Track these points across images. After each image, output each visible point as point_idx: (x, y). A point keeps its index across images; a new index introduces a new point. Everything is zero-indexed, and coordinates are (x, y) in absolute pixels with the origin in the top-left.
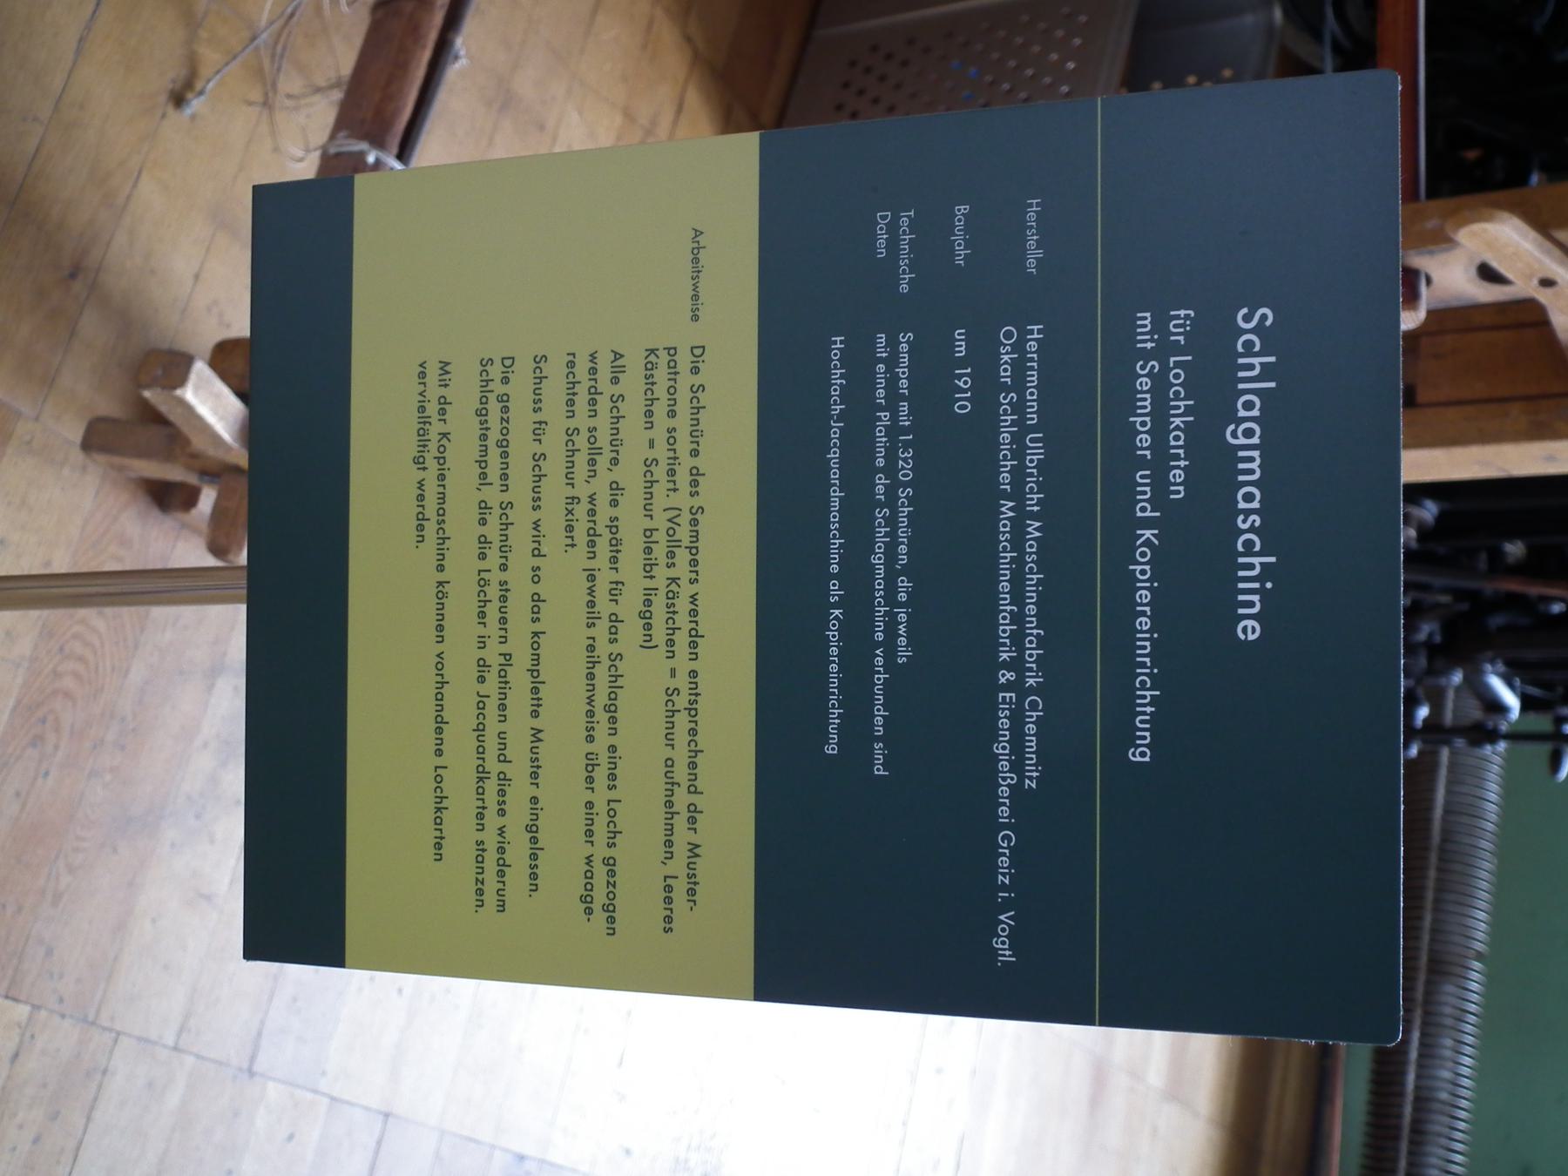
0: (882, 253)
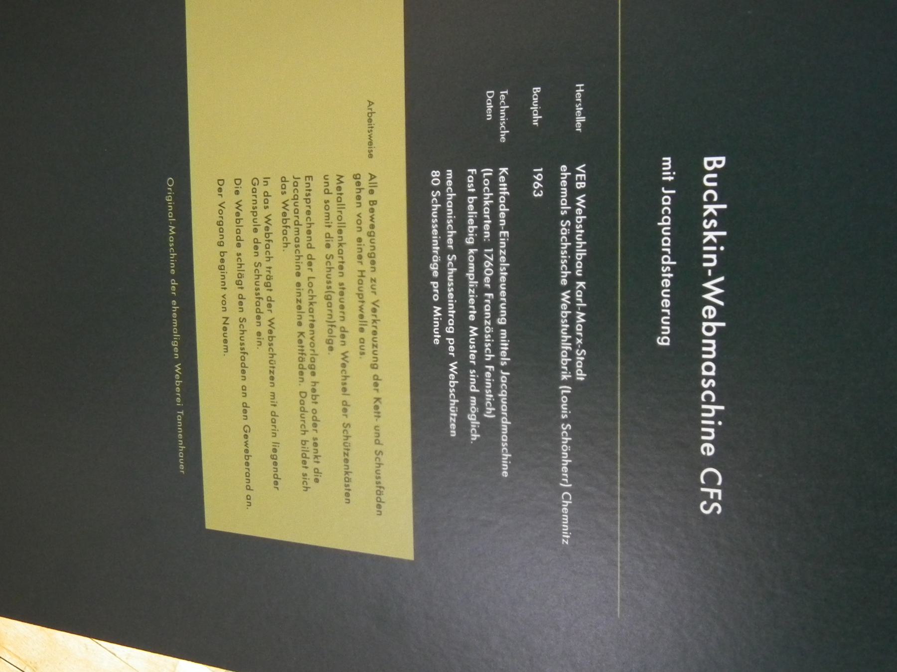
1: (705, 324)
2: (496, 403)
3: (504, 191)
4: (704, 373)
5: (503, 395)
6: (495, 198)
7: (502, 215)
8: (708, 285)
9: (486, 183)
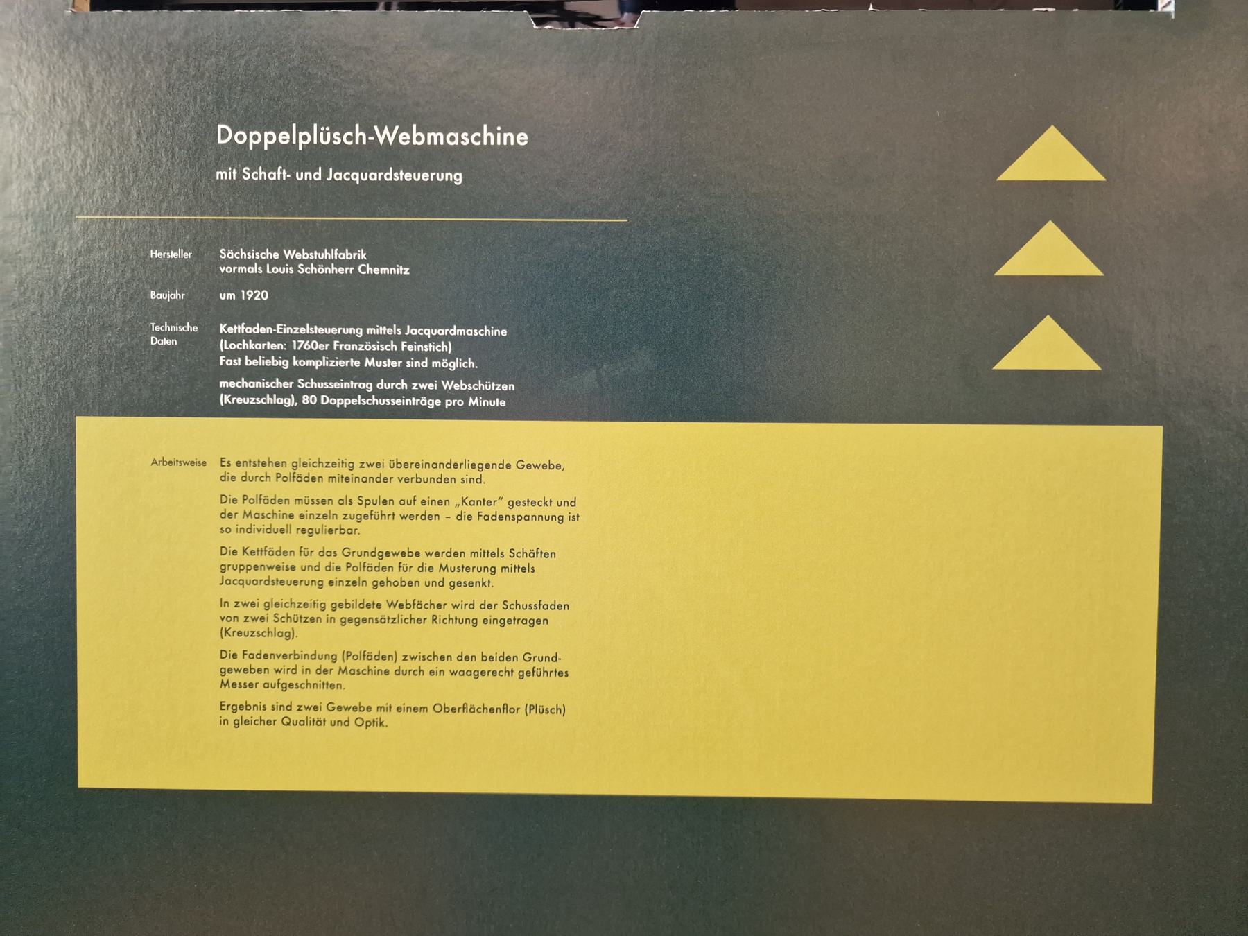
0: (174, 342)
1: (415, 142)
2: (437, 340)
3: (240, 328)
4: (456, 142)
5: (429, 332)
6: (247, 337)
7: (263, 330)
8: (381, 140)
9: (233, 346)
